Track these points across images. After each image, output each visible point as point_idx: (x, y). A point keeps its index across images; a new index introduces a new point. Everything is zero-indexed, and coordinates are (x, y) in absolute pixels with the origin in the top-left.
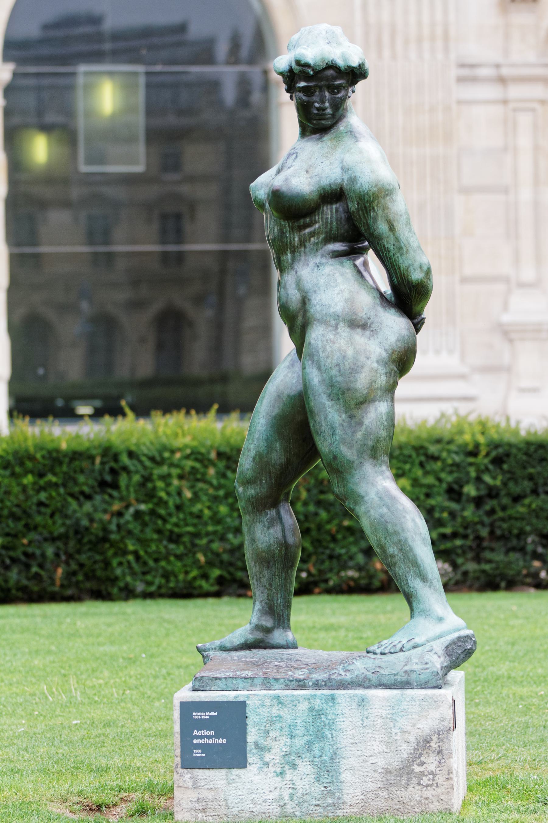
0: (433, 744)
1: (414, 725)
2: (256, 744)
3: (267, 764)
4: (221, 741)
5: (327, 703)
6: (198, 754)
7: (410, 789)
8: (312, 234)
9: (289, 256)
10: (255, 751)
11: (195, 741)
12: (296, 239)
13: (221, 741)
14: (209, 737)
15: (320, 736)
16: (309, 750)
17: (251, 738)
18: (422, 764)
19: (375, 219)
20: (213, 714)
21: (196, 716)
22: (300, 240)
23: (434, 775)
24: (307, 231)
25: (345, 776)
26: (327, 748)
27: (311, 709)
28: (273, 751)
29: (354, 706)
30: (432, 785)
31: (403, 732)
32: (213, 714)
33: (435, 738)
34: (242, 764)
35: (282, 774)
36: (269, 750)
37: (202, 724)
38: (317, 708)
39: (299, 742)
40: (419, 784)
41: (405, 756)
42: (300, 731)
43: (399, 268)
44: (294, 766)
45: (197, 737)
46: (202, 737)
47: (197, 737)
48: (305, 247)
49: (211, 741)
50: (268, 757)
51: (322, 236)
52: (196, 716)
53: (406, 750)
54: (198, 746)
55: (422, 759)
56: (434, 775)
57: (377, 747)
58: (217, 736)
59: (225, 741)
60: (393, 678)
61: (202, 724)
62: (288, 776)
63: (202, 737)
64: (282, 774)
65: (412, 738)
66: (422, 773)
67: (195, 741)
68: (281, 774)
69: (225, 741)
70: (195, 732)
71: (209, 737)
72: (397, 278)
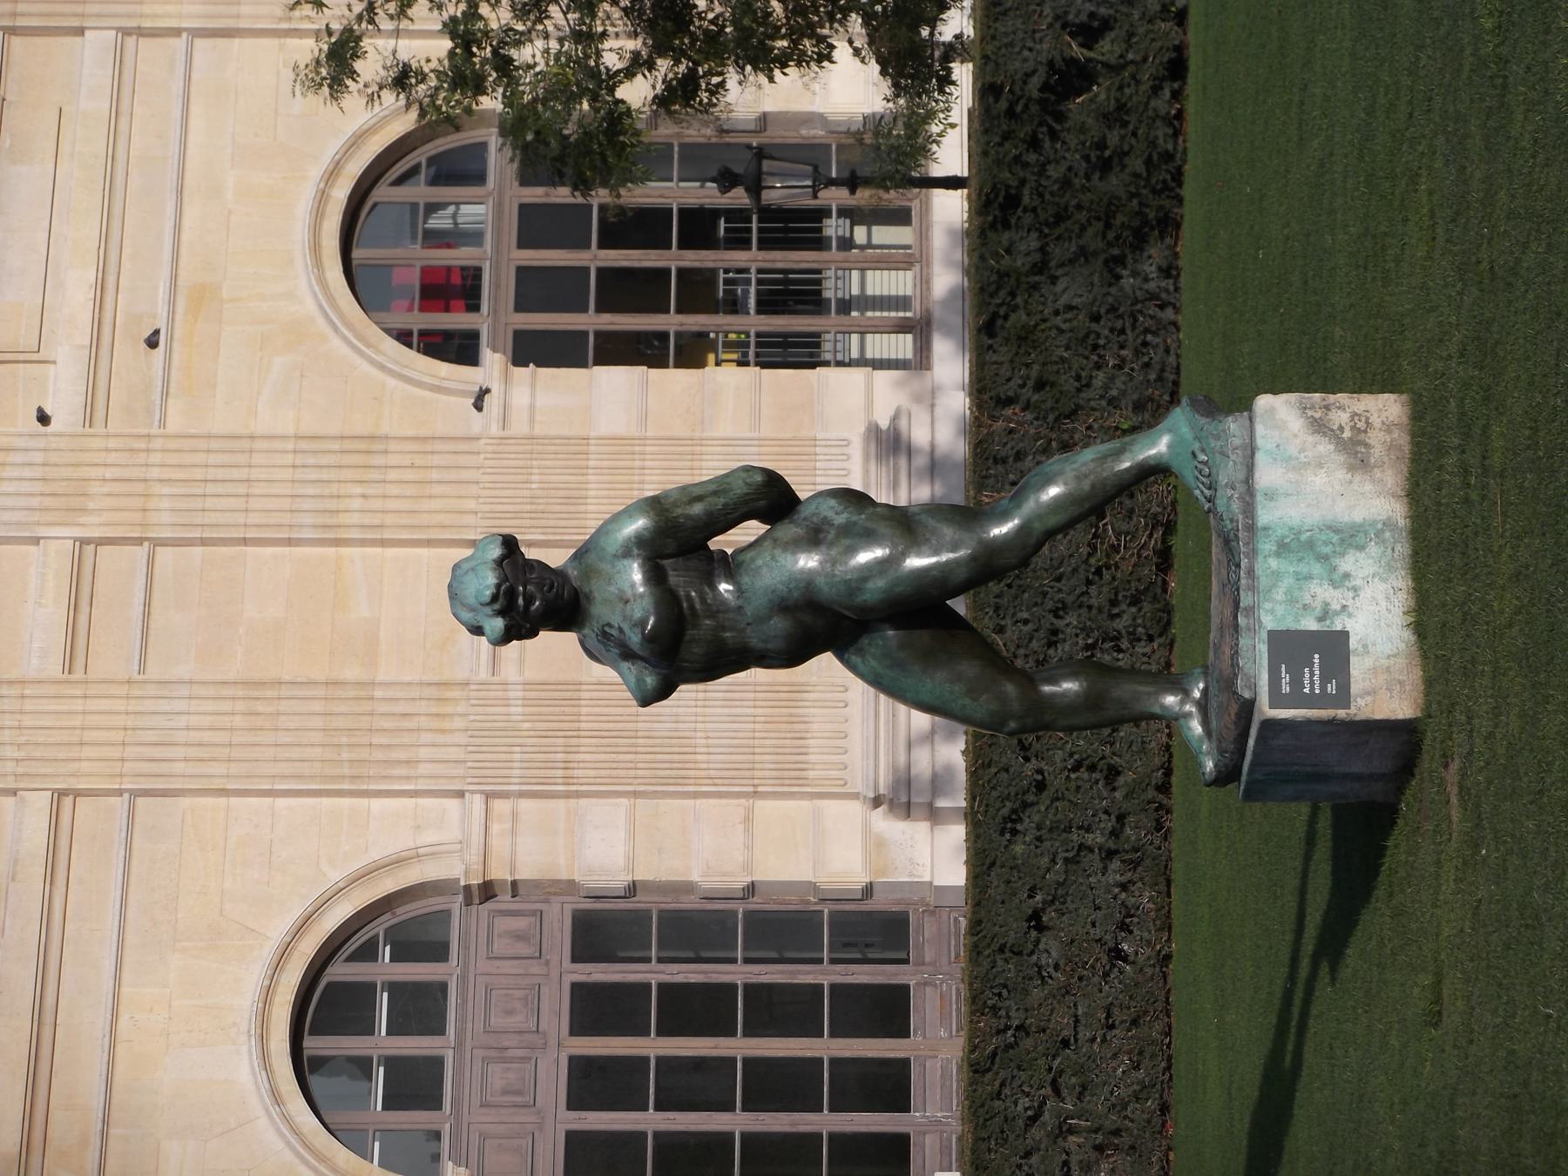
0: (1317, 415)
1: (1296, 436)
2: (1320, 619)
3: (1344, 607)
4: (1316, 661)
5: (1269, 536)
6: (1331, 688)
7: (1371, 442)
8: (703, 600)
9: (727, 634)
10: (1328, 622)
11: (1317, 691)
12: (708, 622)
13: (1316, 661)
14: (1312, 674)
15: (1310, 544)
16: (1326, 558)
17: (1310, 624)
18: (1341, 428)
19: (688, 517)
20: (1283, 669)
21: (1286, 689)
22: (708, 617)
23: (1354, 414)
24: (698, 606)
25: (1358, 516)
26: (1324, 538)
27: (1278, 555)
28: (1328, 600)
29: (1272, 504)
30: (1367, 418)
31: (1302, 450)
32: (1283, 669)
33: (1310, 413)
34: (1345, 635)
35: (1355, 589)
36: (1327, 604)
37: (1297, 682)
38: (1274, 548)
39: (1317, 569)
40: (1365, 432)
41: (1332, 447)
42: (1303, 568)
43: (747, 494)
44: (1347, 576)
45: (1312, 689)
46: (1312, 683)
47: (1312, 689)
48: (718, 612)
49: (1317, 672)
50: (1336, 606)
51: (707, 589)
52: (1286, 689)
53: (1325, 447)
54: (1323, 687)
55: (1335, 428)
56: (1354, 414)
57: (1318, 480)
58: (1311, 666)
59: (1317, 656)
60: (1239, 467)
61: (1297, 682)
62: (1358, 582)
63: (1312, 683)
64: (1355, 589)
65: (1311, 439)
66: (1353, 428)
67: (1317, 691)
68: (1355, 590)
69: (1317, 656)
70: (1307, 690)
71: (1312, 674)
72: (759, 499)
